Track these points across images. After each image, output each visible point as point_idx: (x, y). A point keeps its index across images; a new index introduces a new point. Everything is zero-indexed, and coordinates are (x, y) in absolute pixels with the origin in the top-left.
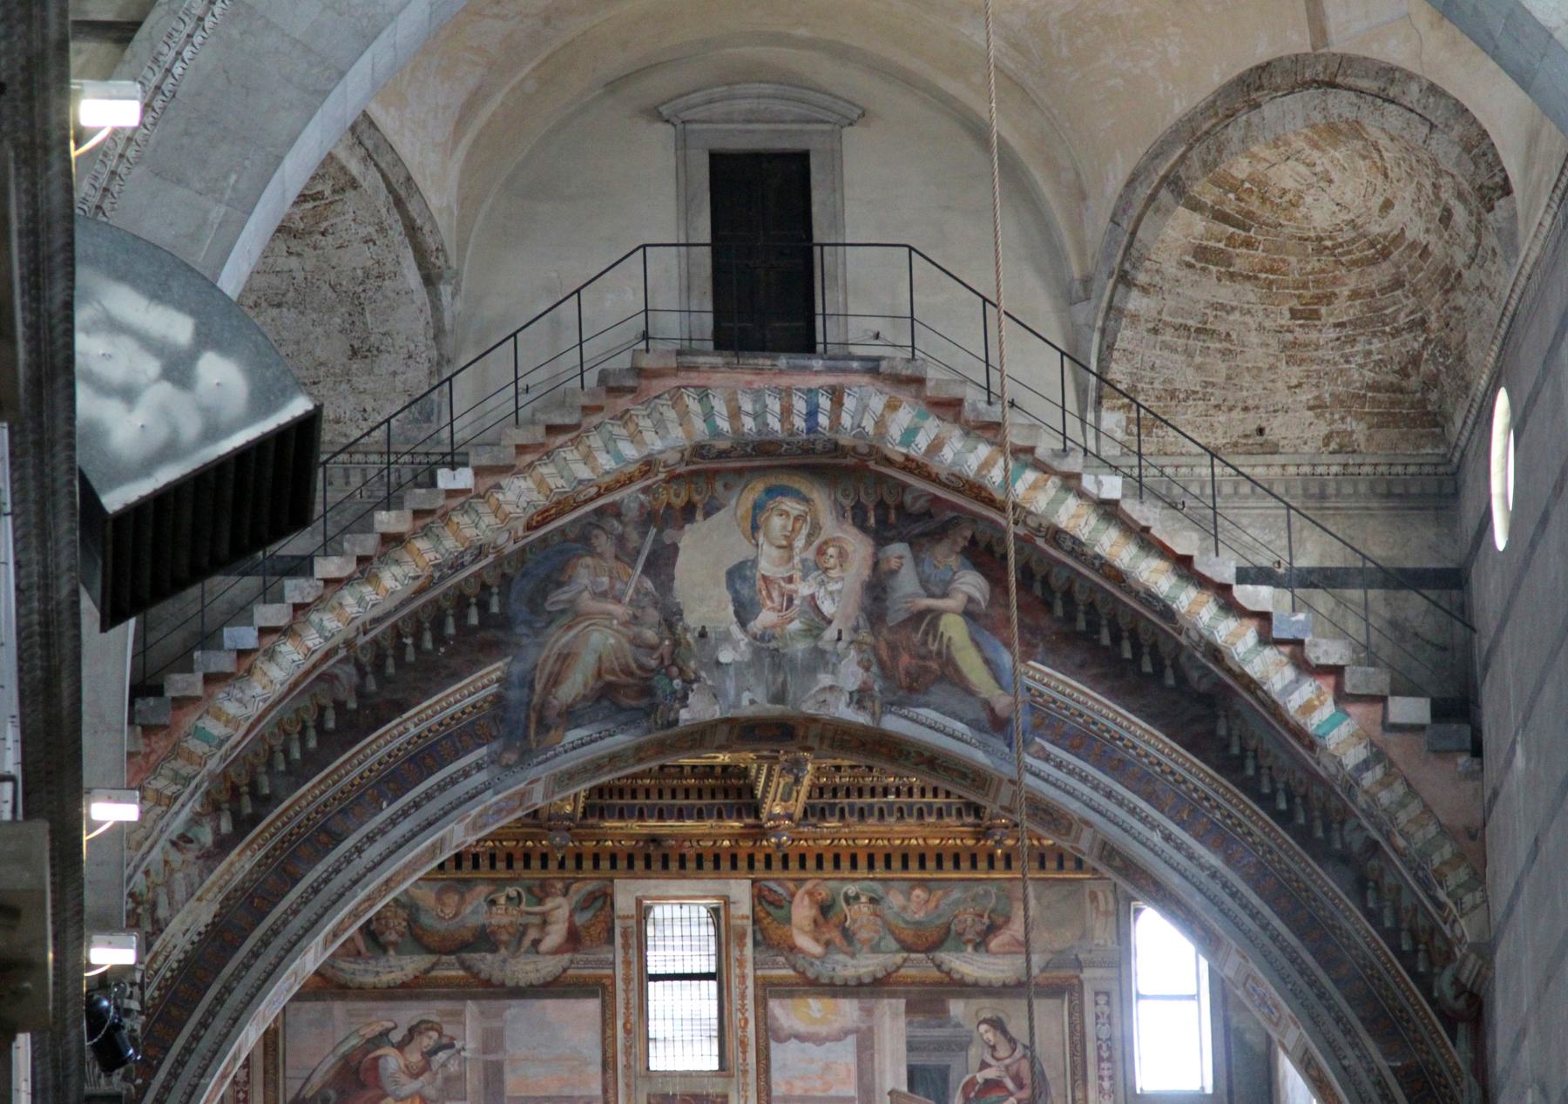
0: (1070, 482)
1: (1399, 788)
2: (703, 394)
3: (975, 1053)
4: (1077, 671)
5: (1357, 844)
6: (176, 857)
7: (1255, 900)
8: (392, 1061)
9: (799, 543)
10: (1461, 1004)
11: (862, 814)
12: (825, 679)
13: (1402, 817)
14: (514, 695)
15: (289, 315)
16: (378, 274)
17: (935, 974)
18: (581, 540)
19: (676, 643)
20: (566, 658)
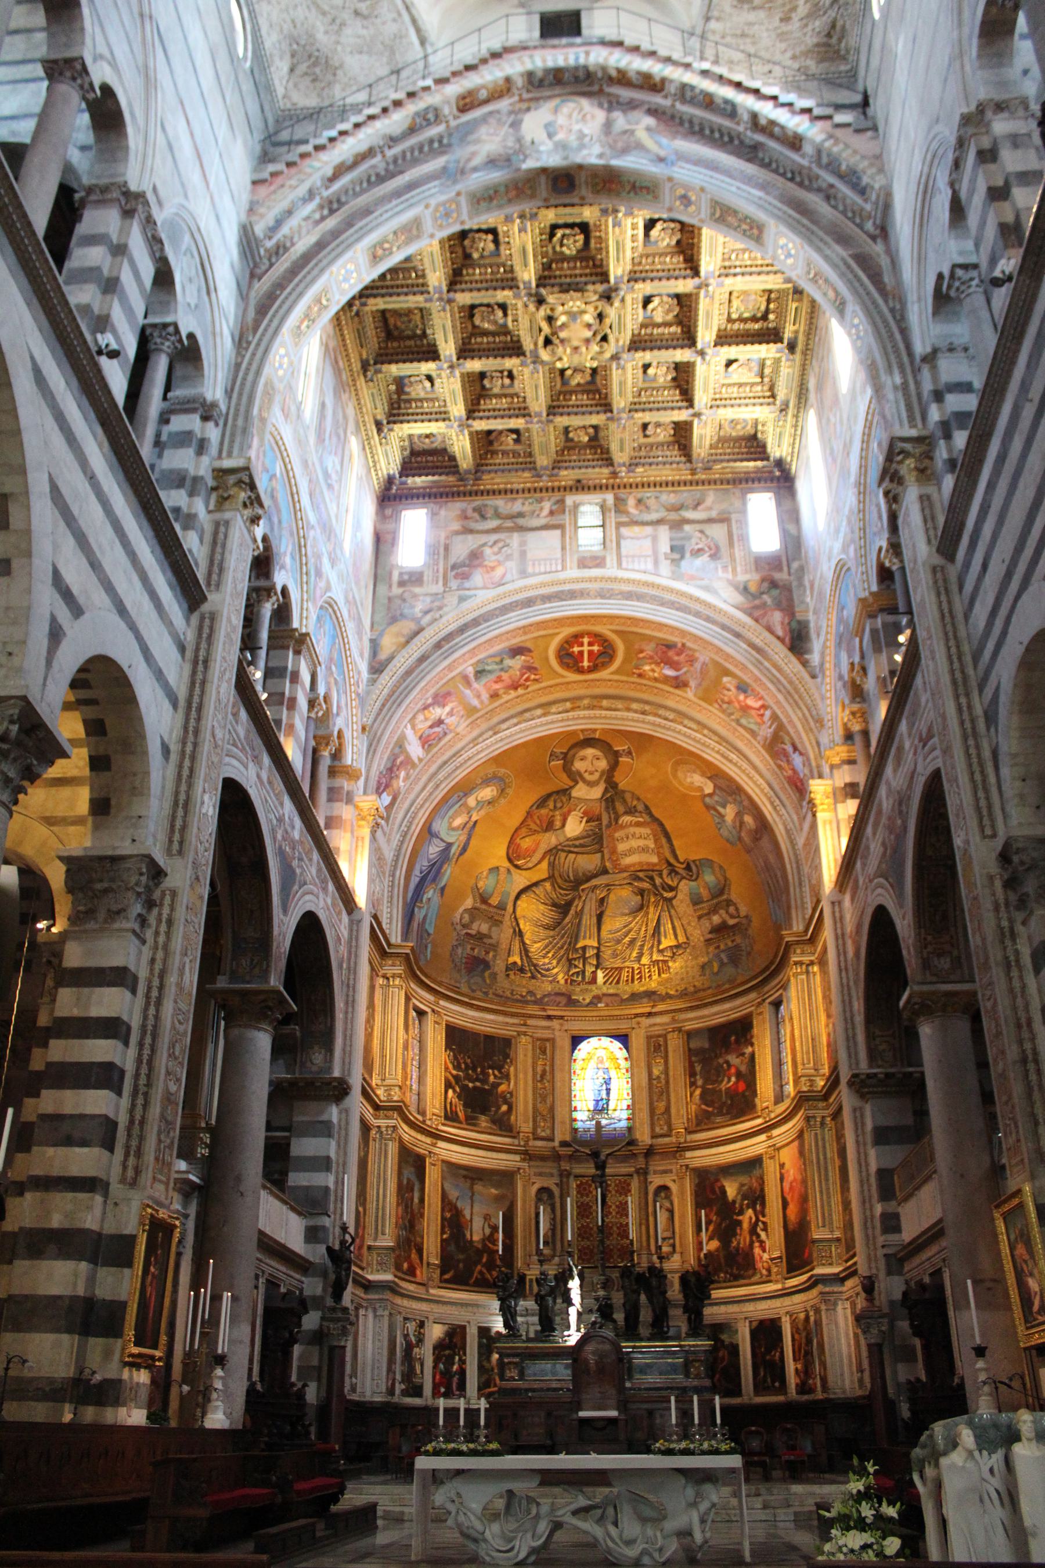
0: (687, 66)
1: (841, 146)
2: (531, 57)
3: (694, 541)
4: (697, 142)
5: (824, 185)
6: (303, 224)
7: (779, 205)
8: (488, 551)
9: (575, 115)
10: (878, 232)
11: (650, 464)
12: (585, 152)
13: (844, 155)
14: (452, 166)
15: (365, 57)
16: (400, 36)
17: (677, 518)
18: (484, 119)
19: (521, 146)
20: (474, 154)
